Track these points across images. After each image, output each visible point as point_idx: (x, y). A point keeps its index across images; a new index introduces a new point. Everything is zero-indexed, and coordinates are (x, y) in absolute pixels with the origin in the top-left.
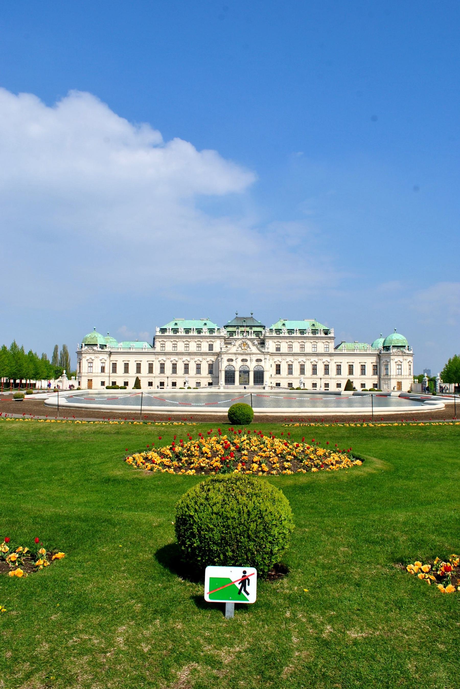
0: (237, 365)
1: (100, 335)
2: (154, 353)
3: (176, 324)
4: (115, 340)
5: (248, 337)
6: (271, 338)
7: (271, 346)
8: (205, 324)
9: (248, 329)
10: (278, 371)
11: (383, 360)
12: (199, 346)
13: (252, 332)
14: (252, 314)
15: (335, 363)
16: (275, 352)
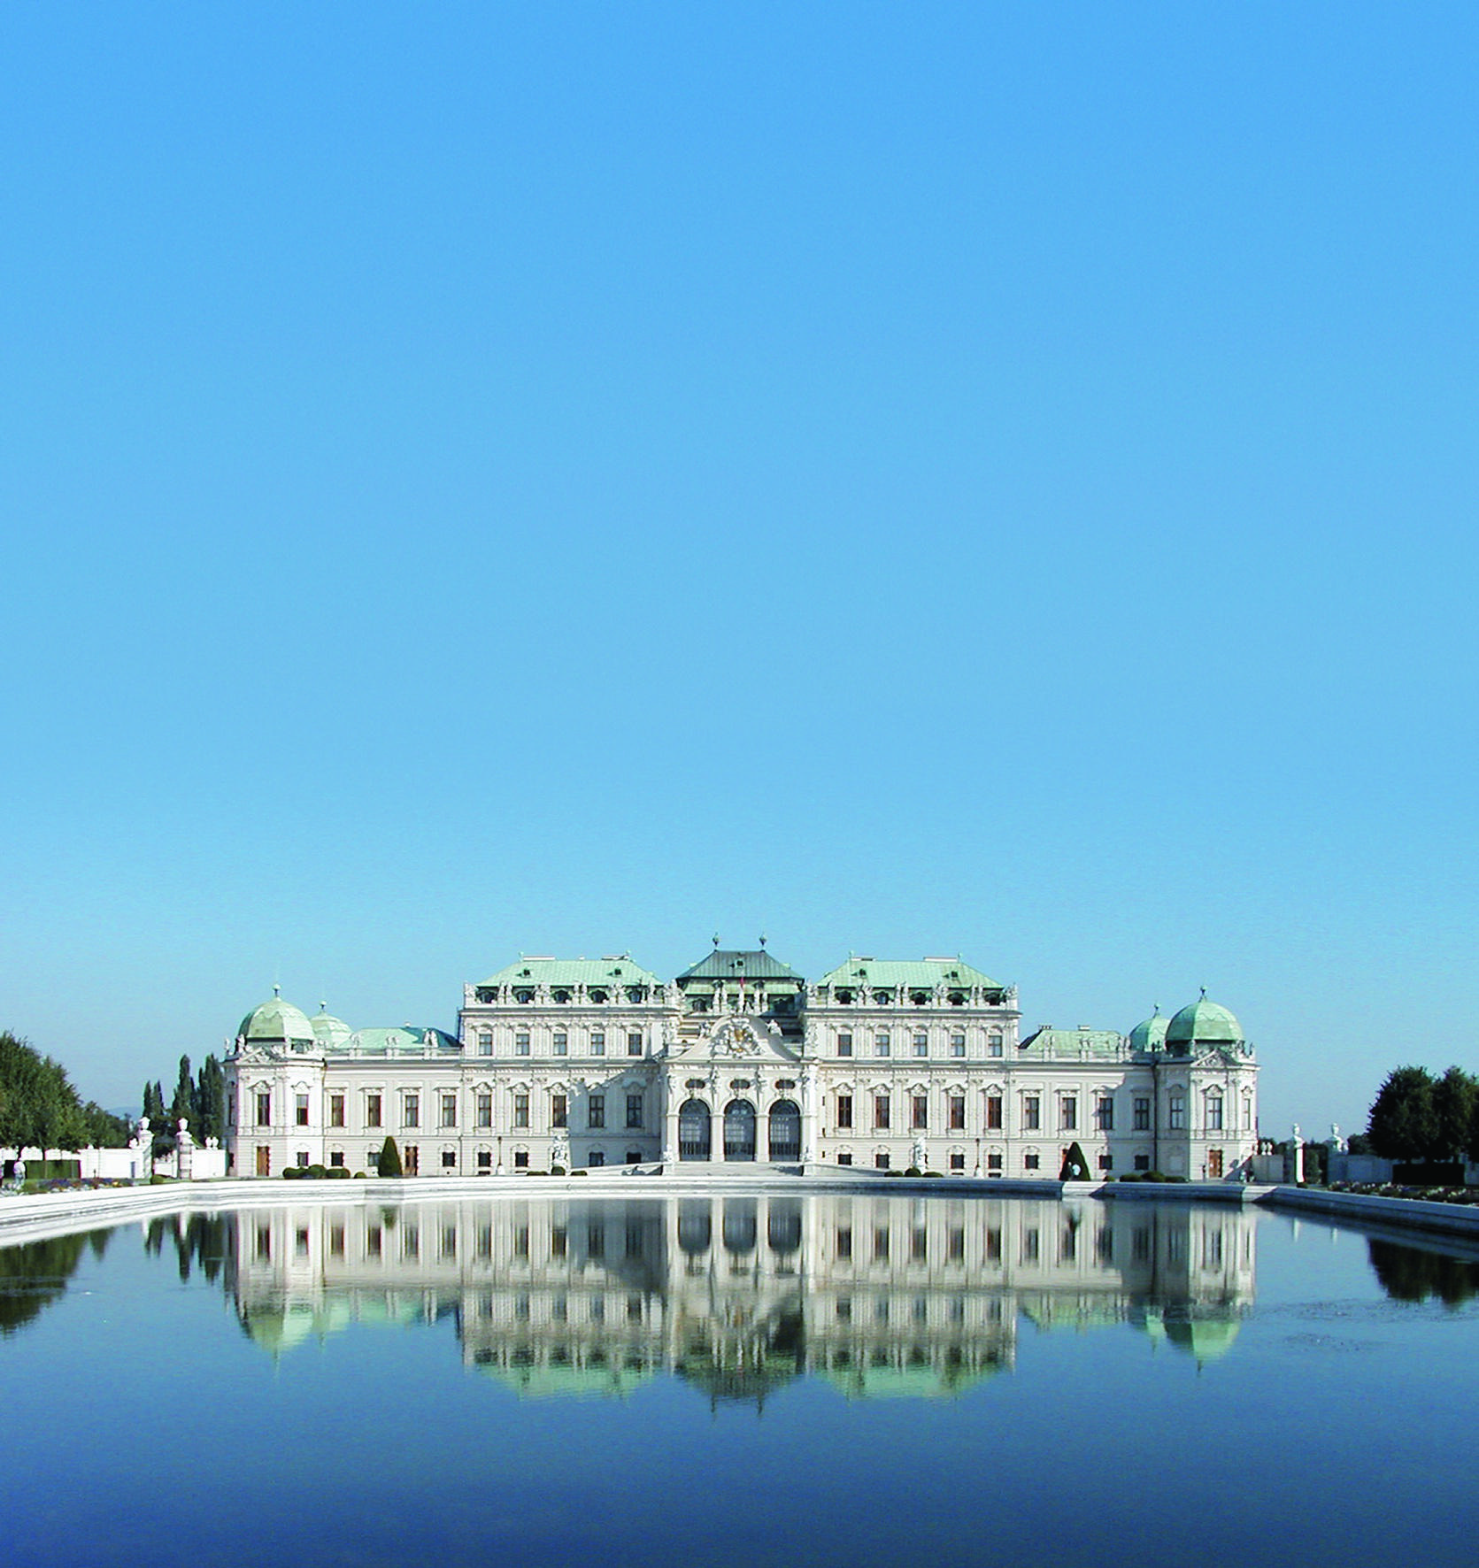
0: (718, 1098)
1: (292, 1011)
2: (458, 1065)
3: (527, 973)
4: (345, 1026)
5: (751, 1012)
6: (824, 1013)
7: (821, 1038)
8: (618, 972)
9: (749, 988)
10: (845, 1118)
11: (1170, 1079)
12: (599, 1042)
13: (765, 996)
14: (763, 942)
15: (1021, 1091)
16: (834, 1056)
